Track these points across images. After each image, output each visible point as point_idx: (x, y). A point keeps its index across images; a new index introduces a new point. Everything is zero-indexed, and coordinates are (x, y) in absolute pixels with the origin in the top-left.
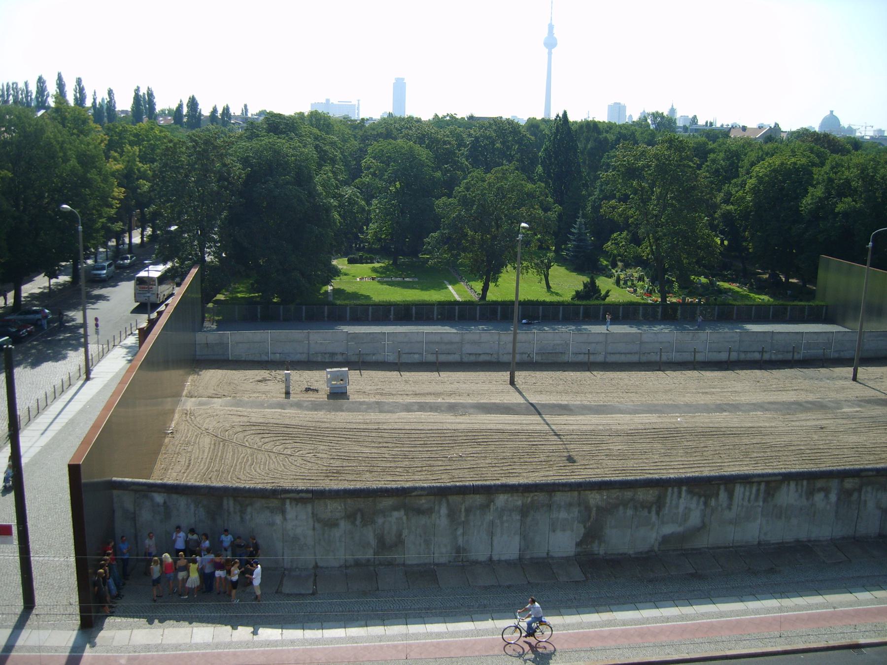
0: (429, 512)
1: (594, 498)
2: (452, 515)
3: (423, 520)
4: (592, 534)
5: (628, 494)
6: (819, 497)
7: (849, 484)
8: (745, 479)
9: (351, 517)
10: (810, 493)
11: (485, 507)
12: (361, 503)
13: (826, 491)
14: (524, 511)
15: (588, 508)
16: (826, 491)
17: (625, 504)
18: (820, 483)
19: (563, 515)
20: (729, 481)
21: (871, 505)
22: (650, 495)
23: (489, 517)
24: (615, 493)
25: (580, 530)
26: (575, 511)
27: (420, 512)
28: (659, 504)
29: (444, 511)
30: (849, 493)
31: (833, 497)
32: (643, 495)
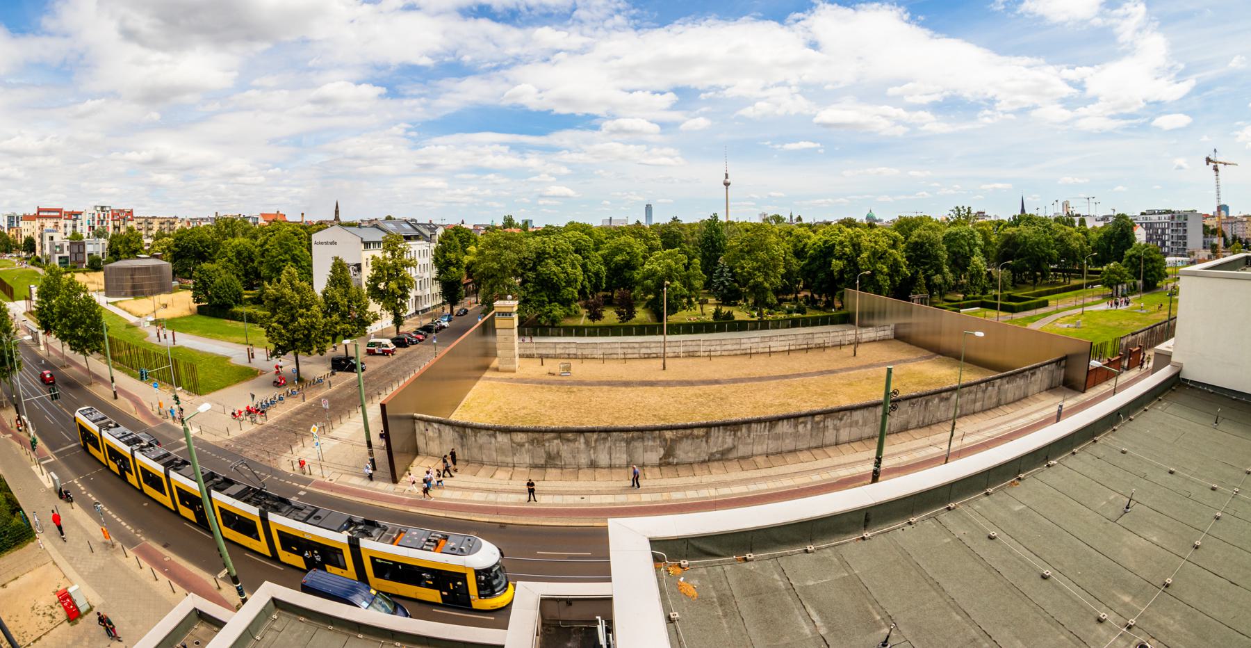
0: (575, 440)
1: (668, 434)
2: (587, 443)
3: (571, 445)
4: (669, 452)
5: (688, 432)
6: (801, 427)
7: (817, 418)
8: (759, 421)
9: (532, 442)
10: (796, 426)
11: (605, 439)
12: (536, 435)
13: (805, 423)
14: (628, 442)
15: (665, 440)
16: (805, 423)
17: (687, 437)
18: (801, 420)
19: (651, 443)
20: (748, 423)
21: (831, 427)
22: (701, 432)
23: (608, 445)
24: (680, 432)
25: (662, 452)
26: (658, 442)
27: (568, 440)
28: (707, 436)
29: (582, 440)
30: (818, 423)
31: (809, 426)
32: (696, 432)
